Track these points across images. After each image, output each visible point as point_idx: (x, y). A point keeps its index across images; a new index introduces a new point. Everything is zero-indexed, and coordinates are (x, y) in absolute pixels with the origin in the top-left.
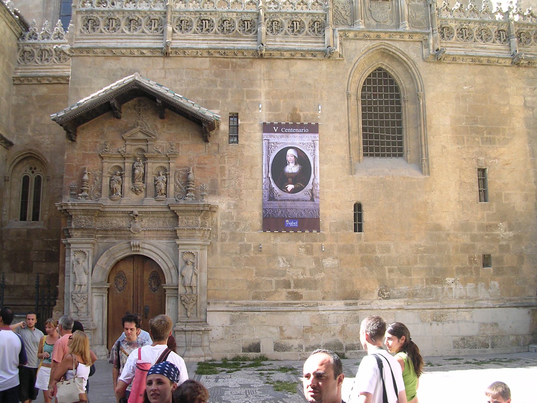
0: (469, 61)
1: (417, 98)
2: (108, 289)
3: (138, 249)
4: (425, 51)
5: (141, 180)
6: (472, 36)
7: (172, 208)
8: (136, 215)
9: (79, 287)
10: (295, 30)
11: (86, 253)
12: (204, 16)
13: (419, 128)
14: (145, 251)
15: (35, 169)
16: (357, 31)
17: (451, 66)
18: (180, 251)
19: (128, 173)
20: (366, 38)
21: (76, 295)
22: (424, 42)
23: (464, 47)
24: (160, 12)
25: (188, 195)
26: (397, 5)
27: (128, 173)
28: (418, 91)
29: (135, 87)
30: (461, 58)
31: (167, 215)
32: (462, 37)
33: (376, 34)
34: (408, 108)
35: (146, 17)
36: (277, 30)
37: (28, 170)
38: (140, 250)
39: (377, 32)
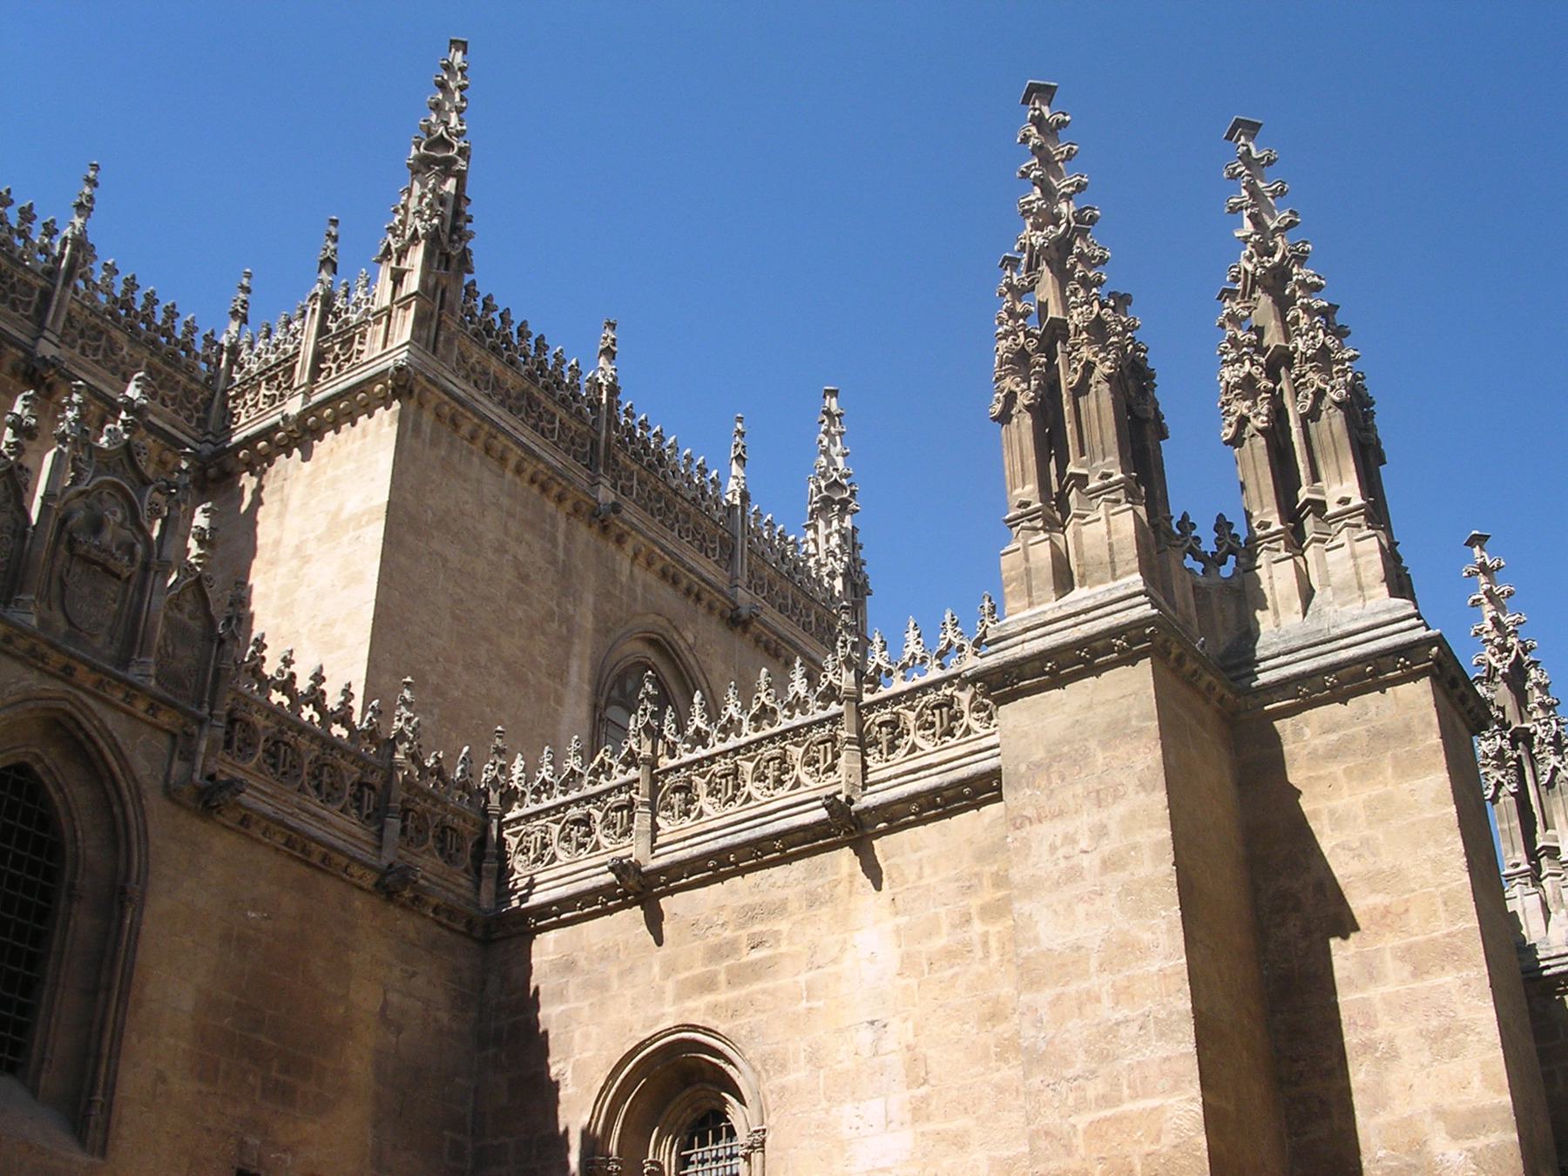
0: (279, 840)
1: (120, 897)
4: (178, 767)
6: (297, 771)
13: (101, 996)
16: (14, 625)
17: (232, 838)
20: (33, 659)
22: (180, 740)
23: (272, 796)
26: (136, 599)
28: (127, 879)
30: (264, 824)
32: (274, 766)
33: (65, 660)
34: (78, 924)
39: (72, 656)
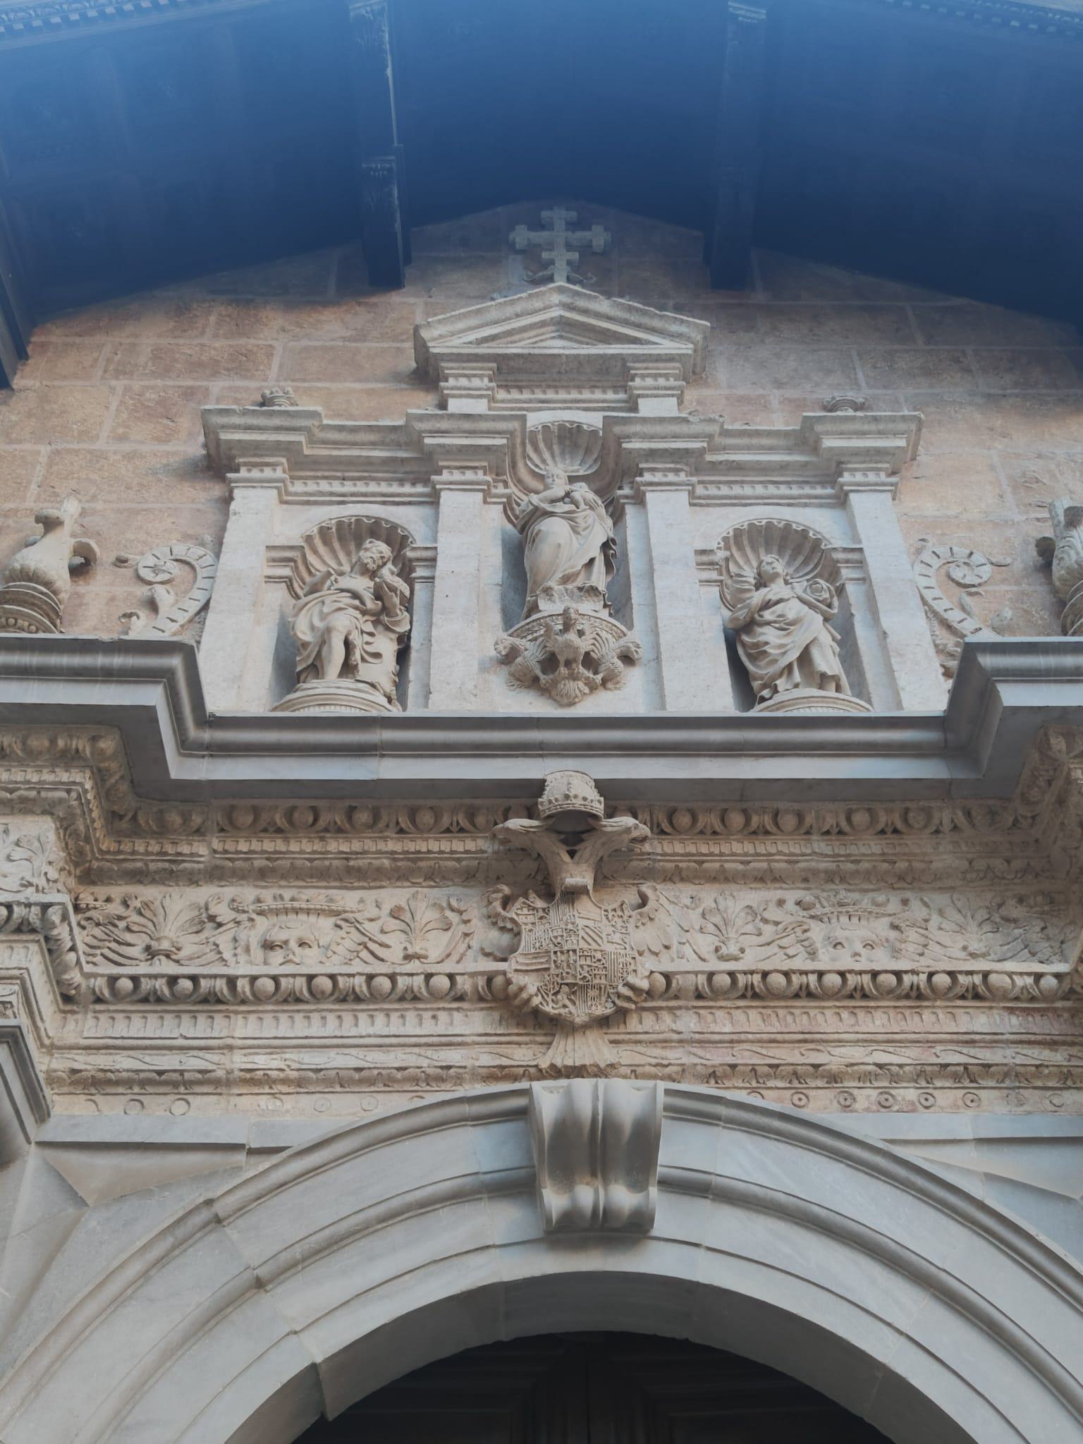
3: (623, 1197)
14: (727, 1226)
31: (918, 844)
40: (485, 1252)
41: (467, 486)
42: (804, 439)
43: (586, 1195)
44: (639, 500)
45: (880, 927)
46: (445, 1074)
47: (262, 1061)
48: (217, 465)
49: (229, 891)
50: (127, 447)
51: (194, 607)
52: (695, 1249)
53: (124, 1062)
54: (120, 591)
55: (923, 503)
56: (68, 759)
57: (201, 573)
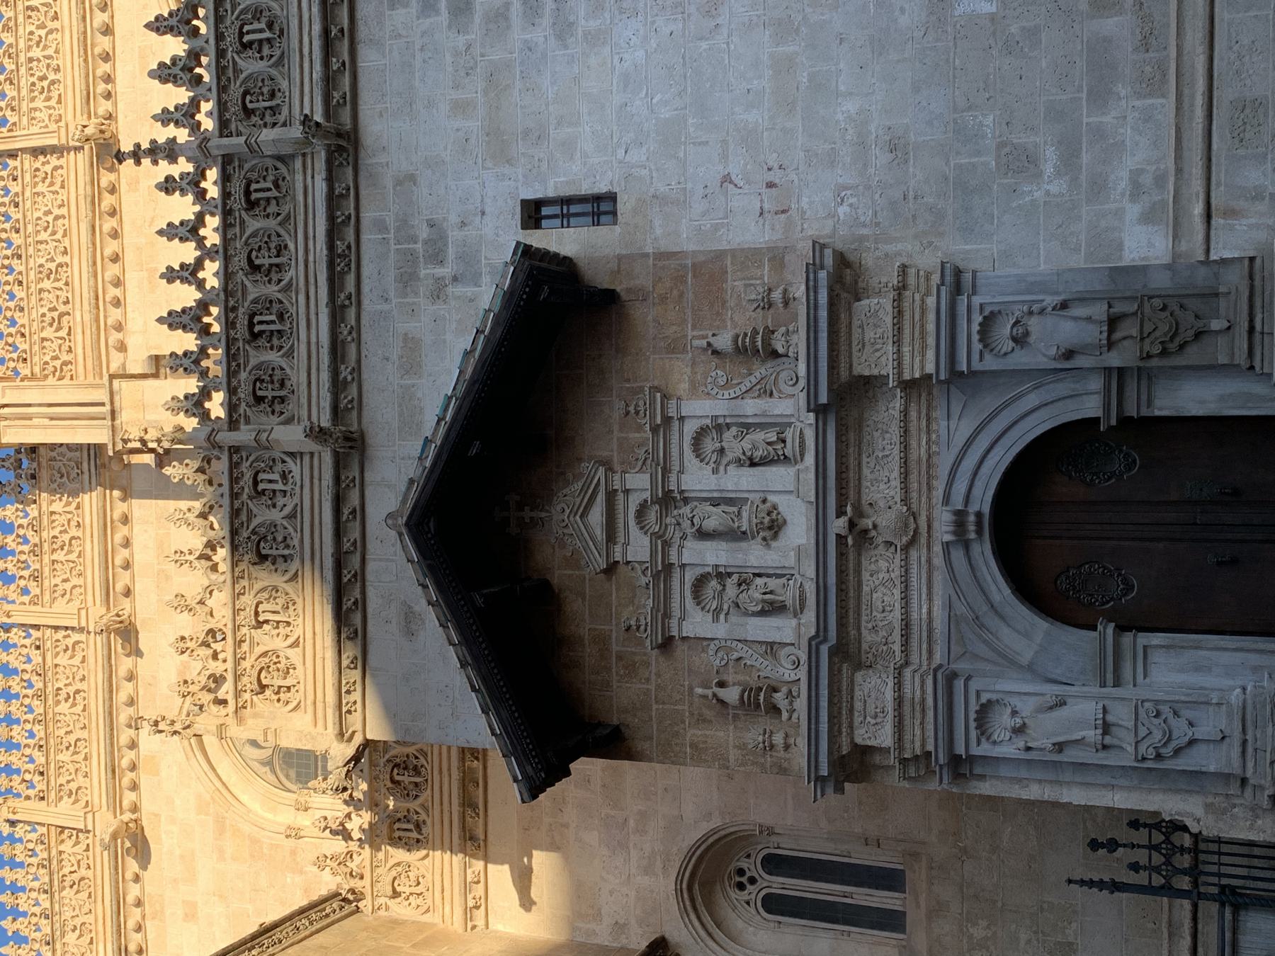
2: (1121, 629)
3: (972, 518)
5: (735, 509)
7: (823, 399)
8: (852, 525)
9: (1114, 729)
10: (267, 35)
11: (983, 700)
12: (241, 330)
14: (977, 492)
15: (741, 872)
18: (977, 366)
19: (714, 554)
21: (1142, 749)
24: (233, 466)
25: (781, 350)
27: (714, 554)
29: (431, 525)
35: (250, 511)
36: (272, 95)
37: (744, 895)
38: (973, 508)
40: (984, 551)
41: (680, 554)
42: (655, 430)
43: (972, 528)
44: (683, 491)
45: (876, 434)
46: (929, 561)
47: (924, 610)
48: (667, 644)
49: (863, 624)
50: (653, 677)
51: (740, 645)
52: (983, 499)
53: (925, 646)
54: (731, 670)
55: (683, 387)
56: (840, 671)
57: (723, 643)
